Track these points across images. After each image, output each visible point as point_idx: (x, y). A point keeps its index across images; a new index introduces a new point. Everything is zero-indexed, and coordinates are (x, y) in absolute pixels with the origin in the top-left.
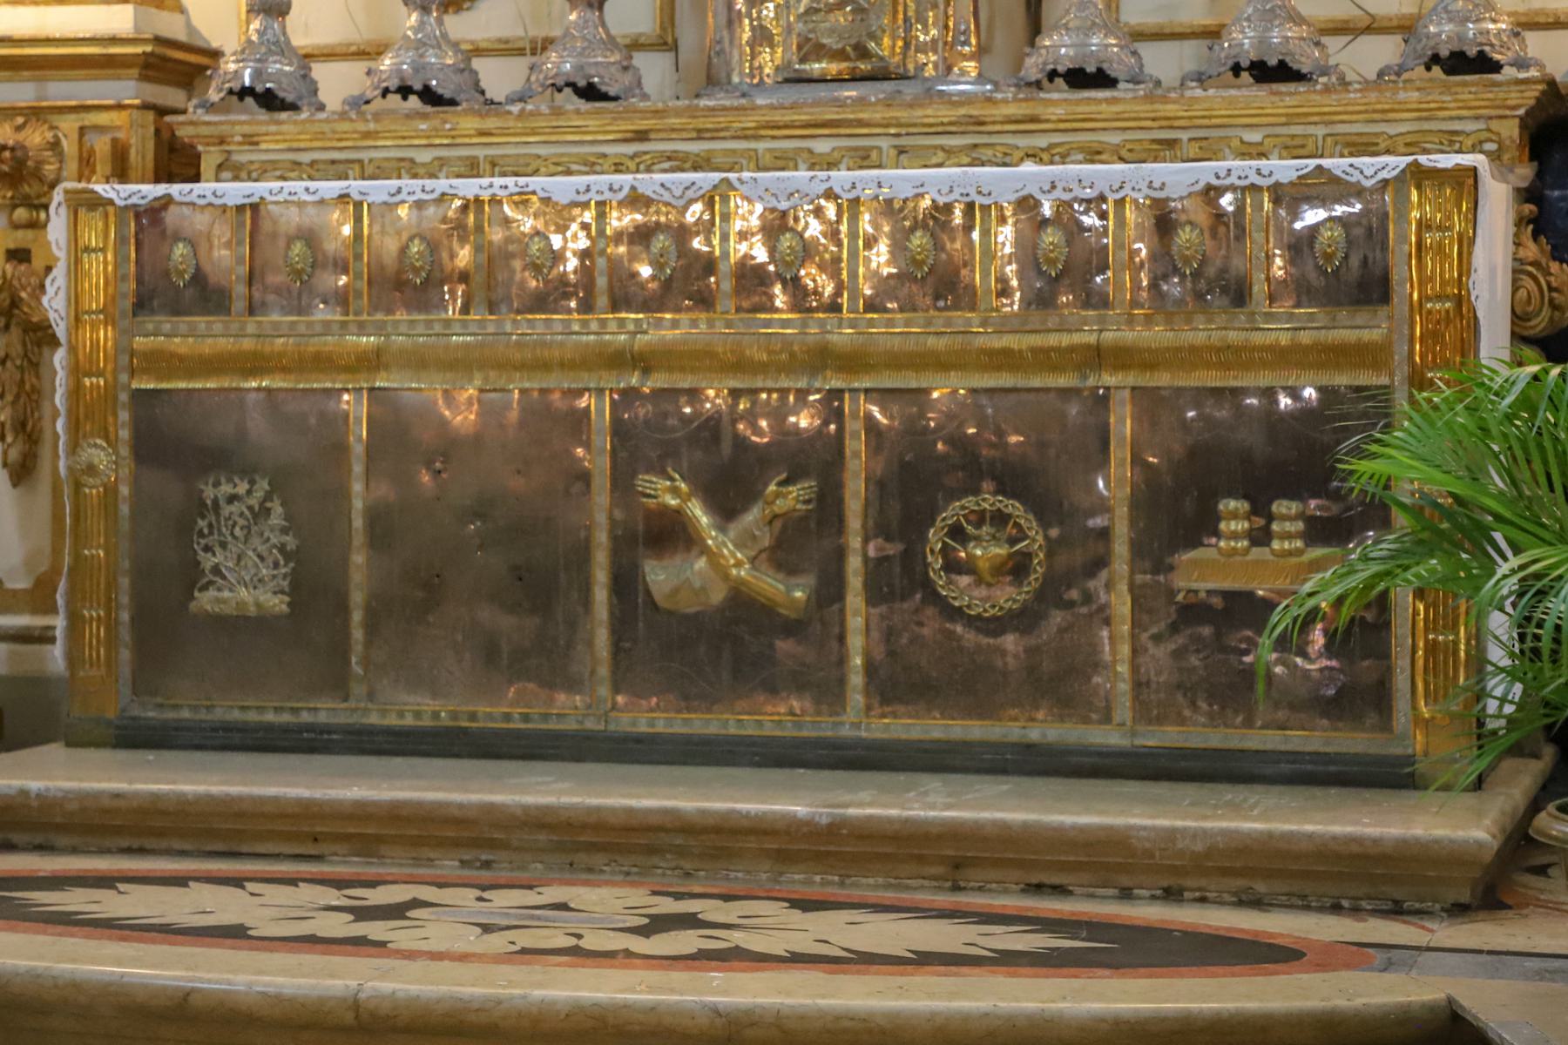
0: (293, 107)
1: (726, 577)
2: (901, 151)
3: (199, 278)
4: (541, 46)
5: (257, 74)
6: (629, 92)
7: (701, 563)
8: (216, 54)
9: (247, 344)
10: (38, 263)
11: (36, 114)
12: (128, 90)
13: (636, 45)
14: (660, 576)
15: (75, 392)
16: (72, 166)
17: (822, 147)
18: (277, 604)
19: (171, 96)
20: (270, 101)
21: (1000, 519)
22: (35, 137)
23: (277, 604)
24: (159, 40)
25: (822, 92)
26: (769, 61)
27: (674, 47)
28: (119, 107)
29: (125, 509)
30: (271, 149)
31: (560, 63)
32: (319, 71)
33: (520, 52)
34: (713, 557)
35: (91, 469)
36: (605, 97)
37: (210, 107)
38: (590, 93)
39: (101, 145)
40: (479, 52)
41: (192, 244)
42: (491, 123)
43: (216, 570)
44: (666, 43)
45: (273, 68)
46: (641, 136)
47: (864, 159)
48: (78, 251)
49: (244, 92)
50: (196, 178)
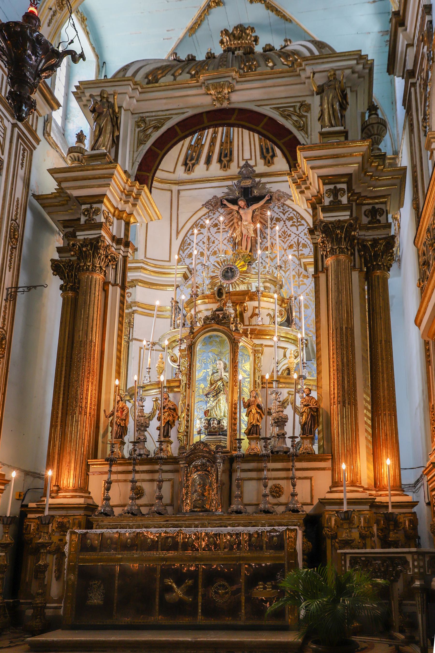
0: (110, 516)
1: (178, 596)
2: (209, 523)
3: (92, 545)
4: (152, 505)
5: (104, 510)
6: (165, 514)
7: (174, 594)
8: (98, 506)
9: (99, 557)
10: (64, 542)
11: (65, 516)
12: (82, 512)
13: (167, 505)
14: (167, 597)
15: (69, 565)
16: (71, 526)
17: (196, 523)
18: (101, 603)
19: (90, 513)
20: (106, 515)
21: (223, 586)
22: (65, 520)
23: (101, 603)
24: (88, 504)
25: (196, 513)
26: (188, 508)
27: (173, 506)
28: (80, 515)
29: (76, 586)
30: (105, 522)
31: (154, 509)
32: (115, 509)
33: (148, 506)
34: (177, 593)
35: (70, 579)
36: (162, 514)
37: (96, 516)
38: (159, 513)
39: (77, 521)
40: (141, 506)
41: (91, 540)
42: (143, 519)
43: (91, 597)
44: (171, 505)
45: (107, 509)
46: (167, 521)
47: (203, 526)
48: (71, 540)
49: (102, 513)
50: (92, 528)
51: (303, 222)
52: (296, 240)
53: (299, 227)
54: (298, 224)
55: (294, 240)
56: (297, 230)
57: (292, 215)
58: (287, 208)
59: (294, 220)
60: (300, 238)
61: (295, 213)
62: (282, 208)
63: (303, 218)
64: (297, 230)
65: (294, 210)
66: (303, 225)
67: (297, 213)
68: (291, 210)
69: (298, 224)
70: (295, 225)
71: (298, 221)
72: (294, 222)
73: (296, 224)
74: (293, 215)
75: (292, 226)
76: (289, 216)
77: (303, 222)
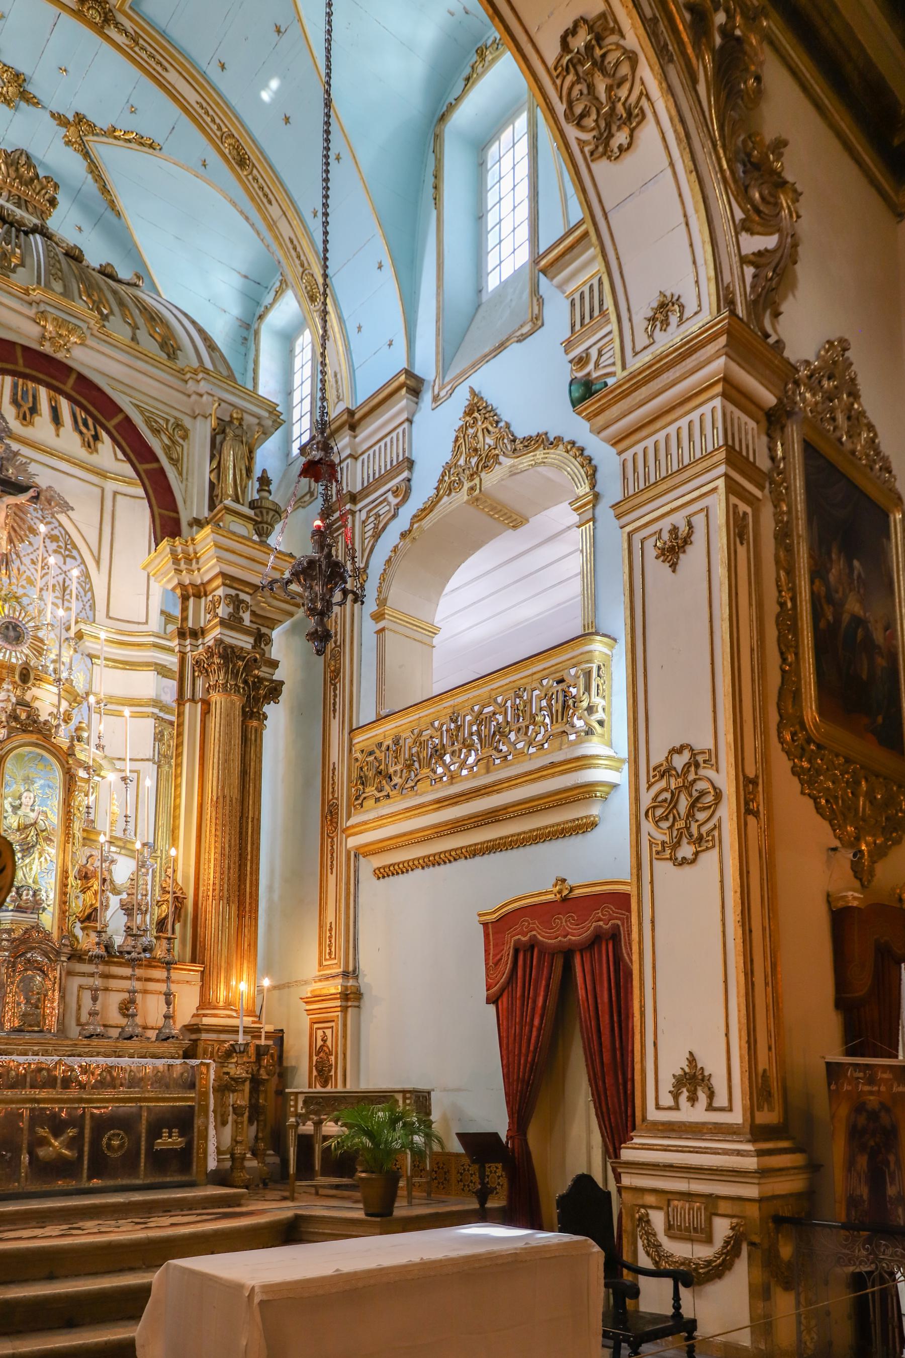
51: (75, 553)
52: (60, 579)
53: (68, 560)
54: (67, 553)
55: (57, 578)
56: (65, 563)
57: (56, 532)
58: (49, 516)
59: (60, 544)
60: (67, 579)
61: (63, 532)
62: (40, 512)
63: (75, 547)
64: (65, 563)
65: (61, 525)
66: (74, 558)
67: (67, 533)
68: (57, 524)
69: (67, 553)
70: (60, 553)
71: (66, 549)
72: (59, 547)
73: (62, 551)
74: (58, 534)
75: (55, 551)
76: (53, 533)
77: (75, 553)
